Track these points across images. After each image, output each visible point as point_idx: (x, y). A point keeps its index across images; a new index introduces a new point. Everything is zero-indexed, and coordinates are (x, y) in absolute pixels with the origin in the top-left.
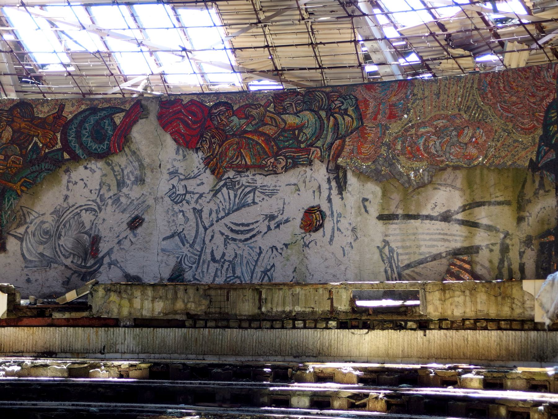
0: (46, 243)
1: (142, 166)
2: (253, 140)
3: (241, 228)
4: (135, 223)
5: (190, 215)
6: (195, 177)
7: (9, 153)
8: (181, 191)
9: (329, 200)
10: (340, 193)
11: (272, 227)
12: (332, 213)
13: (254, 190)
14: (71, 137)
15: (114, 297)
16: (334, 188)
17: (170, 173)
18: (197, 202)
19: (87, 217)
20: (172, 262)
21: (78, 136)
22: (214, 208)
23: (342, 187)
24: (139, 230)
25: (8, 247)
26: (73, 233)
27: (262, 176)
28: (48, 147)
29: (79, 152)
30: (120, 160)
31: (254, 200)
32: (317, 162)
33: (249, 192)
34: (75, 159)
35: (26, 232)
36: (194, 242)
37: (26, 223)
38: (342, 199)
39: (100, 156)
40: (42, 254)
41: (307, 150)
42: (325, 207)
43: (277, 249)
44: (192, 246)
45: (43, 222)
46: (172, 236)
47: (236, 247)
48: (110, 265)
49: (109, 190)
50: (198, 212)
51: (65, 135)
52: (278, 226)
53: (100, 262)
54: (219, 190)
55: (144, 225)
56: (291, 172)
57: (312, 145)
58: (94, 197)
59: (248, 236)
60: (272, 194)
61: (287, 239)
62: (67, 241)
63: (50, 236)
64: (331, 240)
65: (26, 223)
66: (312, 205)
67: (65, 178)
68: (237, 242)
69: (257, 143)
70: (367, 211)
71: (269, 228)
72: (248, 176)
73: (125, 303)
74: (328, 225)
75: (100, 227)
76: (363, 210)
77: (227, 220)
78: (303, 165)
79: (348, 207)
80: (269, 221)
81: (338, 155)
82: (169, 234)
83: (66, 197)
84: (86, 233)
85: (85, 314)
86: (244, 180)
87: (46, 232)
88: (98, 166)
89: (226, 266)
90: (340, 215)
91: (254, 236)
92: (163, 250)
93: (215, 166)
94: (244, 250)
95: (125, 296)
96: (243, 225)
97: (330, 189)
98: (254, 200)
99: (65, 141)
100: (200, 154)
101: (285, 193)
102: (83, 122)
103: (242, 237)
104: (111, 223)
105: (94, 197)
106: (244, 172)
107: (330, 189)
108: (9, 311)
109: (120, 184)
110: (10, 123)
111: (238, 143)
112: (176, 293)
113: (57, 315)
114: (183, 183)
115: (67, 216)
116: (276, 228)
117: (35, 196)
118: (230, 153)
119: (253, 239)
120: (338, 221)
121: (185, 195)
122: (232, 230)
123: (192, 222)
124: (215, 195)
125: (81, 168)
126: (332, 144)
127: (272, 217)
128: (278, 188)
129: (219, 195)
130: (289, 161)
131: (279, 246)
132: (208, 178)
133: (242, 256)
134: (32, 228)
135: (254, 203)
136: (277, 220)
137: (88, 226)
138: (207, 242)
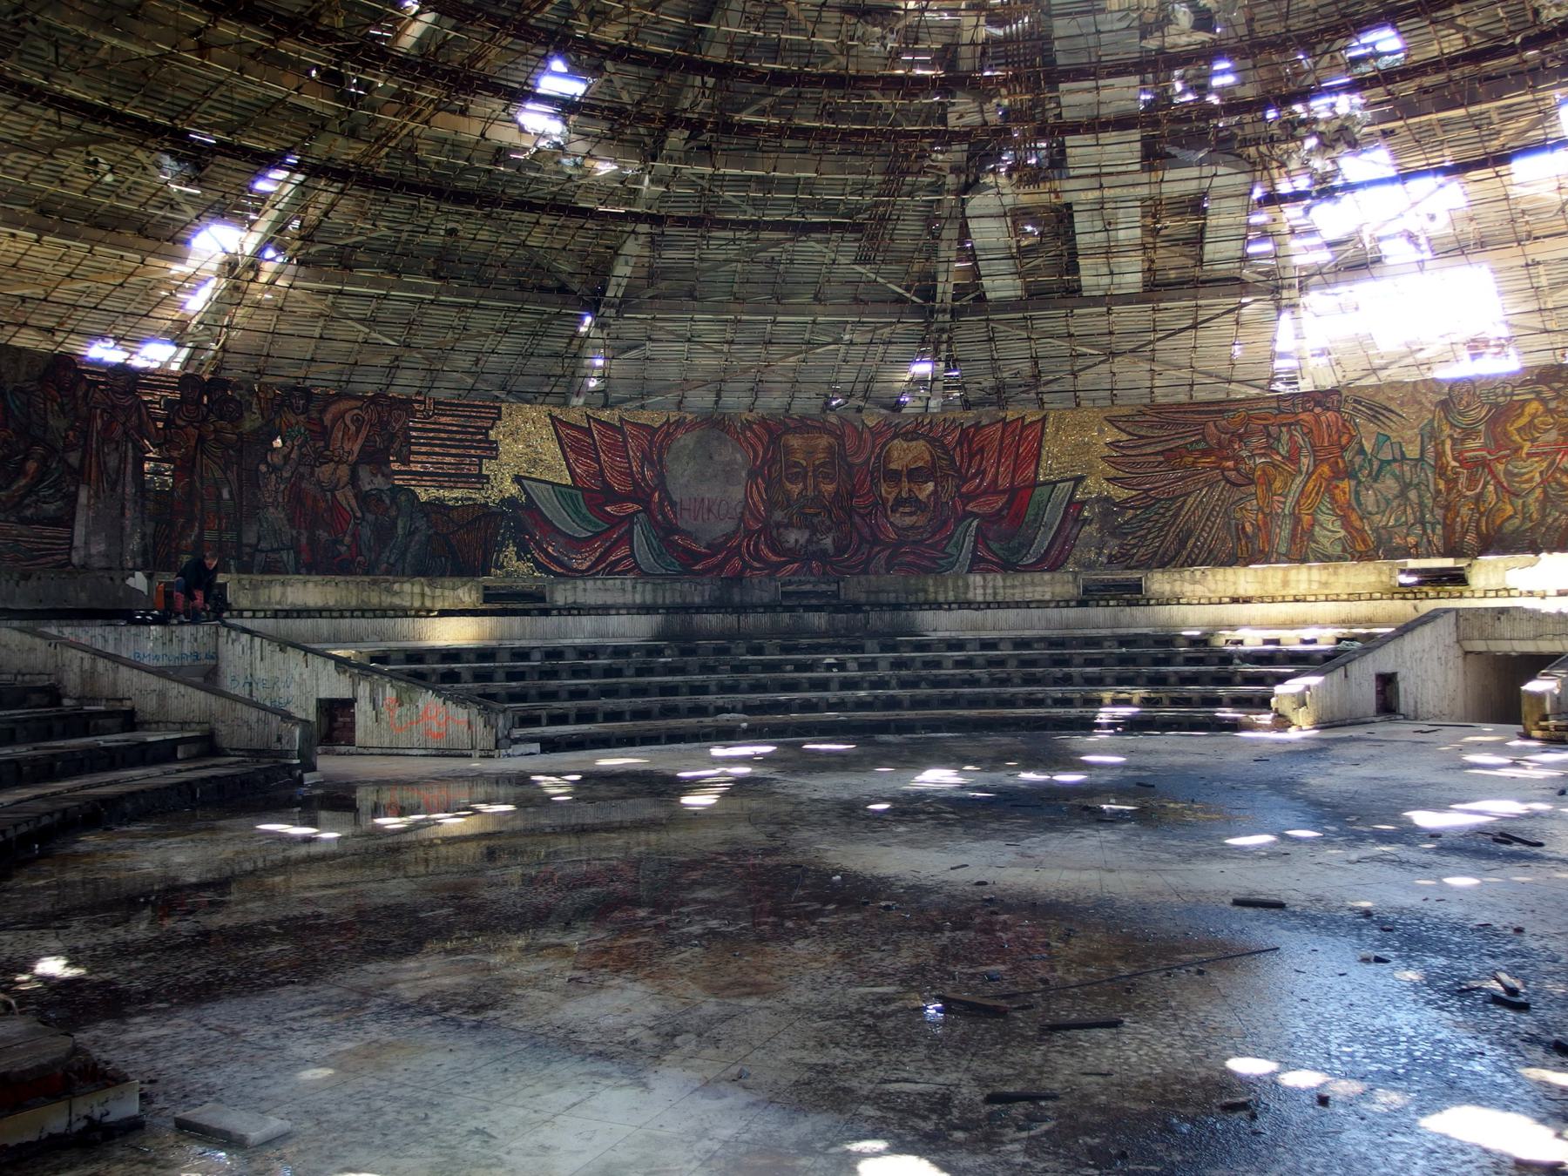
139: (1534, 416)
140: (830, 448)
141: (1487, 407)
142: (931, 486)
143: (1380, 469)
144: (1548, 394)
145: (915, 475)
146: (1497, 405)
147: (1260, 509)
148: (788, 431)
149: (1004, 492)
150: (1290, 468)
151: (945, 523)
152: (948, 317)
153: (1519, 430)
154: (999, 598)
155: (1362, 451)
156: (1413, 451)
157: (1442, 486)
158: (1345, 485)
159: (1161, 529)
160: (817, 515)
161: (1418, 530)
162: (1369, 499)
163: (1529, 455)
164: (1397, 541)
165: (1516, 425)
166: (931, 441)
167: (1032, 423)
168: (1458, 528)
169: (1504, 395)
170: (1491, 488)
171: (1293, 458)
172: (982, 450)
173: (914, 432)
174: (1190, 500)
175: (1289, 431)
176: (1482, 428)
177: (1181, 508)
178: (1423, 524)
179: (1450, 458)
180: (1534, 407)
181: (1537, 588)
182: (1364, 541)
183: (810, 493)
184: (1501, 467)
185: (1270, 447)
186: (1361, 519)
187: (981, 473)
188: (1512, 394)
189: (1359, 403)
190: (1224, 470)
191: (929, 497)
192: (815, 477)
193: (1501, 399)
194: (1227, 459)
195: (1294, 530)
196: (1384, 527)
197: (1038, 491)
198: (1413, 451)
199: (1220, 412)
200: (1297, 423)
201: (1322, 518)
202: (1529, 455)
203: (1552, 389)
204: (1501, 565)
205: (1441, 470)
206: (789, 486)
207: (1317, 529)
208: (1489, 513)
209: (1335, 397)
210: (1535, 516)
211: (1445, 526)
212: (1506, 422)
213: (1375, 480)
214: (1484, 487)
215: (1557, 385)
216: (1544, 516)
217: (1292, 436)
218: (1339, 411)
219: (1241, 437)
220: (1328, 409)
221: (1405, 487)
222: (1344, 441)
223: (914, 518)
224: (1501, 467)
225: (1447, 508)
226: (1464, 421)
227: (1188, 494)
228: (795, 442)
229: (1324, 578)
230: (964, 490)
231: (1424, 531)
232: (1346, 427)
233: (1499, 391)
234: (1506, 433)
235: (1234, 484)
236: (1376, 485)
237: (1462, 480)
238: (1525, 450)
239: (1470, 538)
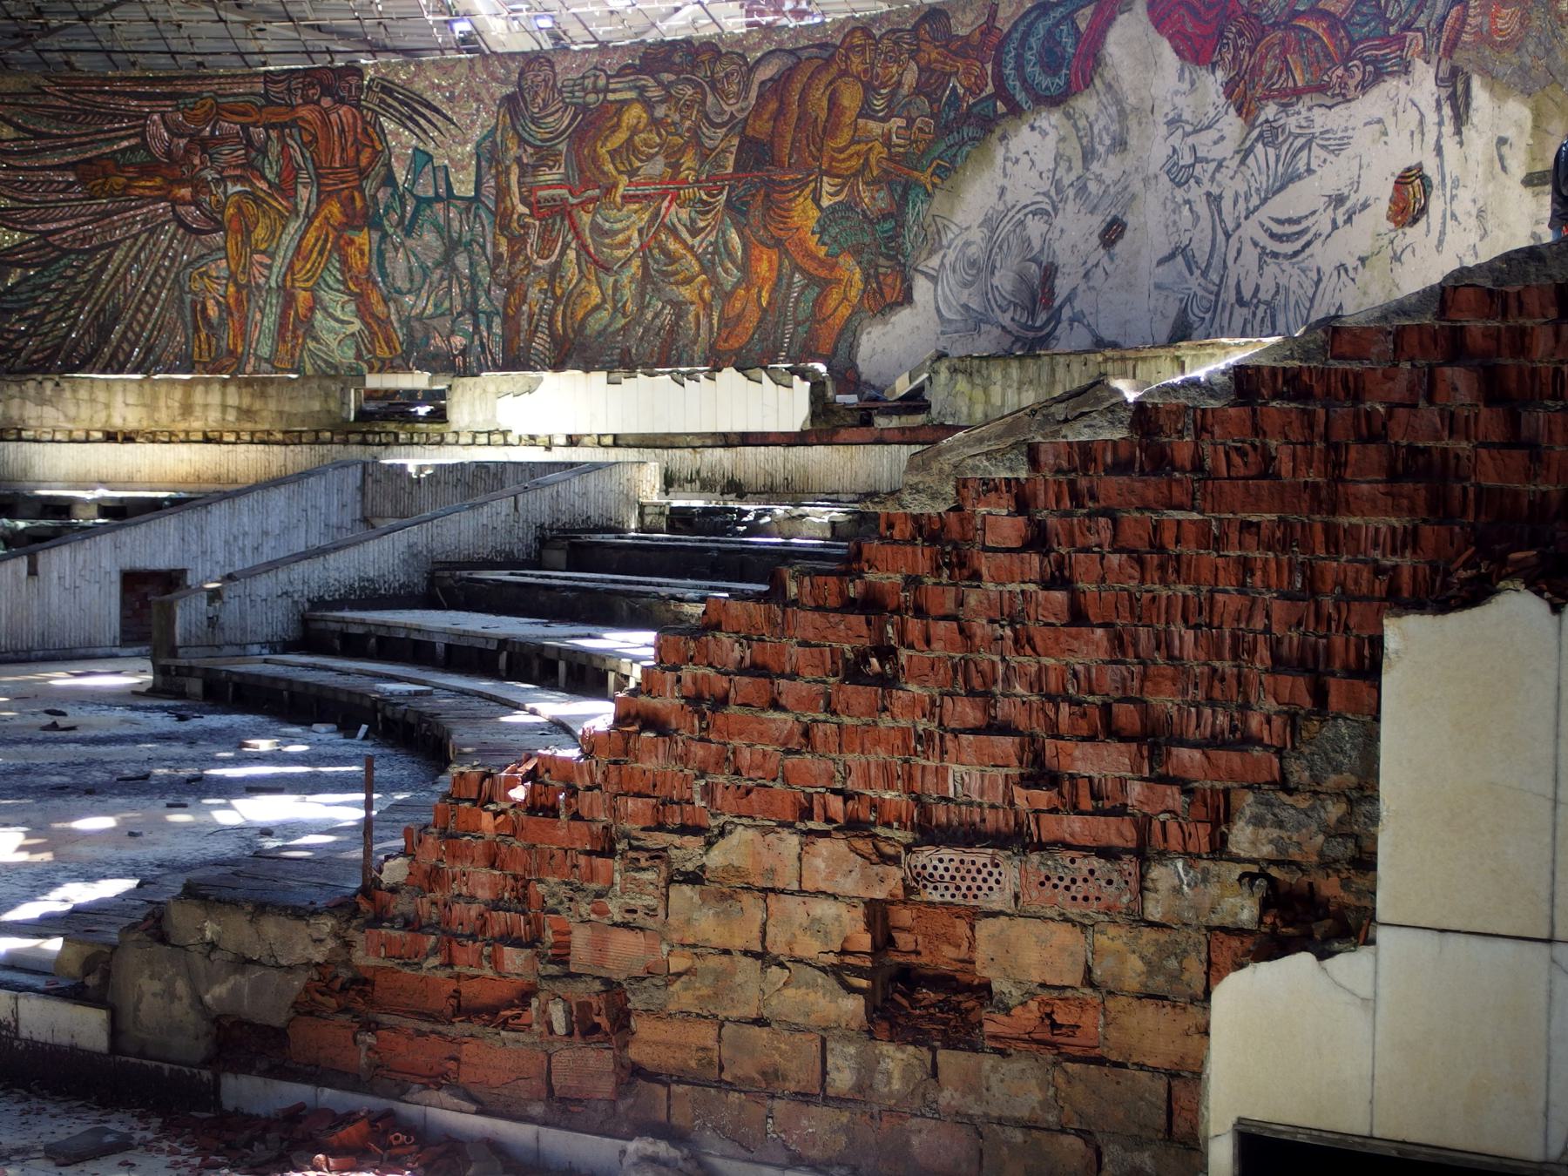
0: (972, 284)
1: (1122, 114)
2: (1307, 30)
3: (1289, 229)
4: (1113, 232)
5: (1202, 208)
6: (1209, 127)
7: (914, 114)
8: (1187, 159)
9: (1439, 150)
10: (1458, 132)
11: (1340, 221)
12: (1443, 179)
13: (1308, 145)
14: (1008, 71)
15: (962, 384)
16: (1447, 120)
17: (1169, 123)
18: (1212, 179)
19: (1035, 228)
20: (1173, 311)
21: (1020, 66)
22: (1242, 188)
23: (1461, 118)
24: (1119, 247)
25: (916, 296)
26: (1013, 262)
27: (1323, 110)
28: (972, 93)
29: (1020, 96)
30: (1087, 104)
31: (1308, 164)
32: (1419, 64)
33: (1301, 149)
34: (1015, 110)
35: (942, 264)
36: (1209, 265)
37: (941, 247)
38: (1461, 143)
39: (1056, 100)
40: (966, 307)
41: (1399, 40)
42: (1430, 170)
43: (1346, 271)
44: (1204, 274)
45: (967, 244)
46: (1172, 256)
47: (1277, 270)
48: (1071, 321)
49: (1070, 169)
50: (1214, 200)
51: (999, 64)
52: (1349, 220)
53: (1055, 317)
54: (1250, 150)
55: (1128, 234)
56: (1376, 93)
57: (1408, 27)
58: (1045, 185)
59: (1298, 245)
60: (1338, 147)
61: (1363, 246)
62: (1004, 280)
63: (980, 269)
64: (1440, 242)
65: (941, 247)
66: (1407, 165)
67: (1000, 153)
68: (1280, 260)
69: (1317, 37)
70: (1504, 168)
71: (1335, 226)
72: (1299, 113)
73: (978, 394)
74: (1436, 205)
75: (1056, 246)
76: (1498, 165)
77: (1263, 215)
78: (1391, 74)
79: (1472, 164)
80: (1336, 208)
81: (1453, 44)
82: (1166, 251)
83: (1003, 191)
84: (1033, 260)
85: (920, 419)
86: (1292, 123)
87: (973, 264)
88: (1051, 120)
89: (1260, 313)
90: (1456, 183)
91: (1308, 244)
92: (1158, 286)
93: (1242, 98)
94: (1290, 275)
95: (978, 381)
96: (1290, 221)
97: (1440, 124)
98: (1308, 164)
99: (999, 80)
100: (1220, 74)
101: (1363, 139)
103: (1288, 248)
104: (1074, 233)
105: (1045, 185)
106: (1292, 105)
107: (1440, 124)
108: (814, 415)
109: (1088, 155)
110: (913, 56)
111: (1282, 41)
112: (1053, 371)
113: (881, 422)
114: (1190, 140)
115: (1006, 228)
116: (1346, 222)
117: (954, 193)
118: (1268, 68)
119: (1308, 251)
120: (1453, 198)
121: (1193, 165)
122: (1272, 236)
123: (1205, 223)
124: (1243, 162)
125: (1025, 129)
126: (1444, 18)
127: (1339, 200)
128: (1350, 133)
129: (1251, 161)
130: (1370, 68)
131: (1351, 262)
132: (1232, 125)
133: (1287, 289)
134: (951, 255)
135: (1310, 171)
136: (1348, 204)
137: (1037, 244)
138: (1230, 262)
139: (634, 131)
141: (571, 111)
144: (654, 93)
146: (584, 108)
147: (232, 276)
150: (280, 204)
153: (613, 154)
155: (390, 180)
156: (464, 186)
157: (503, 249)
158: (363, 238)
159: (69, 305)
162: (399, 264)
163: (627, 199)
164: (437, 342)
165: (609, 146)
168: (524, 324)
169: (596, 91)
170: (572, 254)
171: (285, 187)
174: (118, 255)
175: (281, 138)
176: (563, 147)
177: (102, 268)
178: (475, 315)
179: (516, 201)
180: (634, 114)
181: (541, 432)
182: (388, 341)
184: (586, 218)
185: (249, 165)
186: (386, 301)
188: (606, 90)
189: (390, 92)
190: (175, 202)
193: (591, 98)
194: (181, 183)
195: (284, 315)
196: (419, 317)
198: (464, 186)
200: (293, 123)
201: (326, 296)
202: (627, 199)
203: (660, 83)
204: (491, 388)
205: (502, 219)
207: (319, 315)
208: (568, 300)
209: (353, 80)
210: (630, 307)
211: (506, 319)
212: (595, 139)
213: (408, 234)
214: (563, 253)
215: (667, 77)
216: (642, 308)
217: (285, 147)
218: (358, 106)
219: (205, 145)
220: (342, 101)
221: (452, 246)
222: (364, 161)
224: (586, 218)
225: (510, 286)
226: (539, 134)
227: (116, 245)
229: (246, 402)
231: (476, 326)
232: (370, 138)
233: (589, 83)
234: (595, 159)
235: (188, 228)
236: (409, 242)
237: (533, 238)
238: (621, 190)
239: (541, 342)
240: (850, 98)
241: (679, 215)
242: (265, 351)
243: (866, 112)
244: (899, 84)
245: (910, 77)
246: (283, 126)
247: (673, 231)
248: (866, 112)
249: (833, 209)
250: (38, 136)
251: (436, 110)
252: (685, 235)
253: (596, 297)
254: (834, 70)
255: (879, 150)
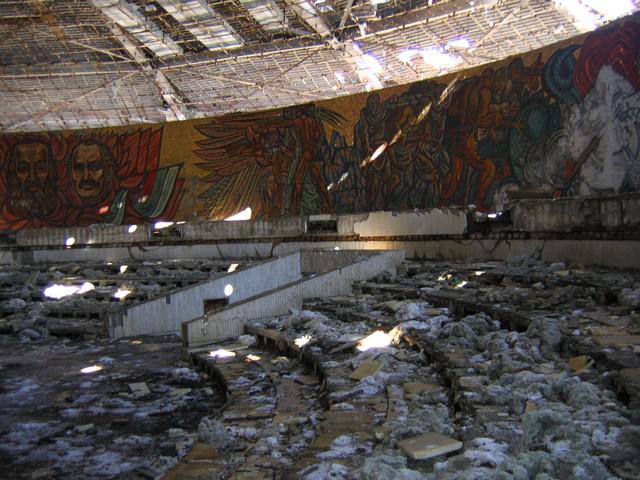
8: (625, 109)
14: (548, 79)
46: (621, 151)
51: (543, 76)
75: (572, 150)
102: (553, 64)
121: (628, 112)
140: (44, 151)
142: (100, 171)
143: (335, 153)
145: (92, 166)
147: (276, 181)
148: (19, 142)
149: (141, 174)
150: (290, 154)
151: (109, 193)
152: (149, 68)
154: (105, 241)
158: (317, 164)
160: (36, 191)
161: (353, 192)
166: (101, 145)
167: (156, 132)
169: (394, 103)
170: (388, 164)
171: (291, 148)
172: (128, 150)
173: (91, 140)
182: (328, 201)
183: (33, 178)
185: (280, 141)
187: (128, 163)
190: (256, 156)
191: (99, 179)
192: (35, 169)
194: (258, 149)
197: (159, 173)
199: (255, 120)
203: (417, 98)
204: (352, 219)
206: (20, 175)
207: (304, 193)
210: (410, 183)
215: (419, 96)
216: (414, 184)
219: (264, 135)
222: (317, 136)
223: (91, 192)
228: (23, 149)
230: (119, 173)
240: (487, 95)
241: (425, 147)
242: (287, 207)
243: (493, 101)
244: (505, 89)
245: (509, 84)
246: (288, 127)
247: (424, 154)
248: (493, 101)
249: (482, 140)
250: (214, 138)
251: (340, 116)
252: (428, 155)
253: (398, 181)
254: (479, 87)
255: (498, 116)
